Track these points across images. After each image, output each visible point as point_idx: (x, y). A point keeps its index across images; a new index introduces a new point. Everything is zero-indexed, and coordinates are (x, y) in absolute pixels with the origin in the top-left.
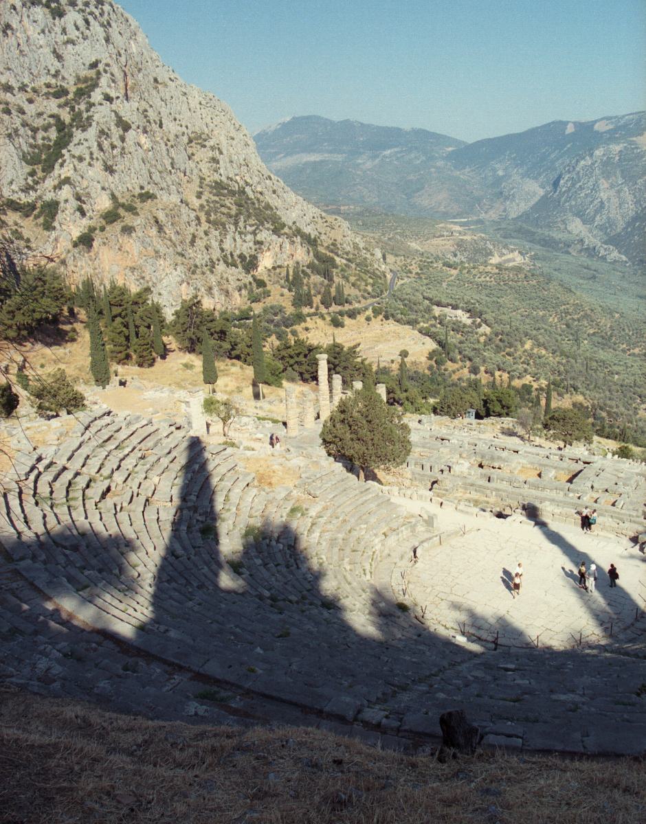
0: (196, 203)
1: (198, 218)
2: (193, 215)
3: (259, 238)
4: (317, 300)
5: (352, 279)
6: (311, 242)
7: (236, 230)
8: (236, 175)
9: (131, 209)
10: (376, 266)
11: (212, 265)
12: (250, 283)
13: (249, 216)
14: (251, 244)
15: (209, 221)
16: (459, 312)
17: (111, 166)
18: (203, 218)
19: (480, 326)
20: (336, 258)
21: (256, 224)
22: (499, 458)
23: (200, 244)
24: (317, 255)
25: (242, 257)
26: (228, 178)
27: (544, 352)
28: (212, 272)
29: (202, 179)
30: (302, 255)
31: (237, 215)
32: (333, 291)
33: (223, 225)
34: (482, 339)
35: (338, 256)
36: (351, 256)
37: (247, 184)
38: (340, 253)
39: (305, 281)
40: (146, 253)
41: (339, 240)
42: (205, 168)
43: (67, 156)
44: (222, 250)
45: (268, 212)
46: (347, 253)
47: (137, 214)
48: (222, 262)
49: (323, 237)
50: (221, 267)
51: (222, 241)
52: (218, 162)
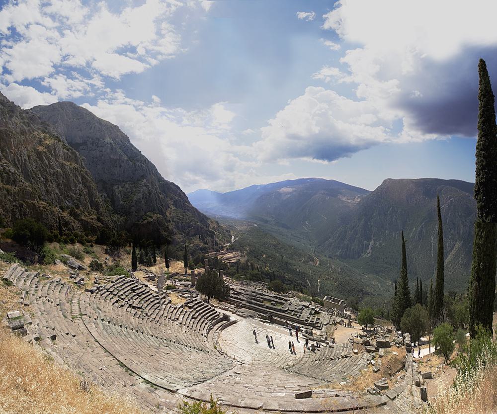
5: (220, 238)
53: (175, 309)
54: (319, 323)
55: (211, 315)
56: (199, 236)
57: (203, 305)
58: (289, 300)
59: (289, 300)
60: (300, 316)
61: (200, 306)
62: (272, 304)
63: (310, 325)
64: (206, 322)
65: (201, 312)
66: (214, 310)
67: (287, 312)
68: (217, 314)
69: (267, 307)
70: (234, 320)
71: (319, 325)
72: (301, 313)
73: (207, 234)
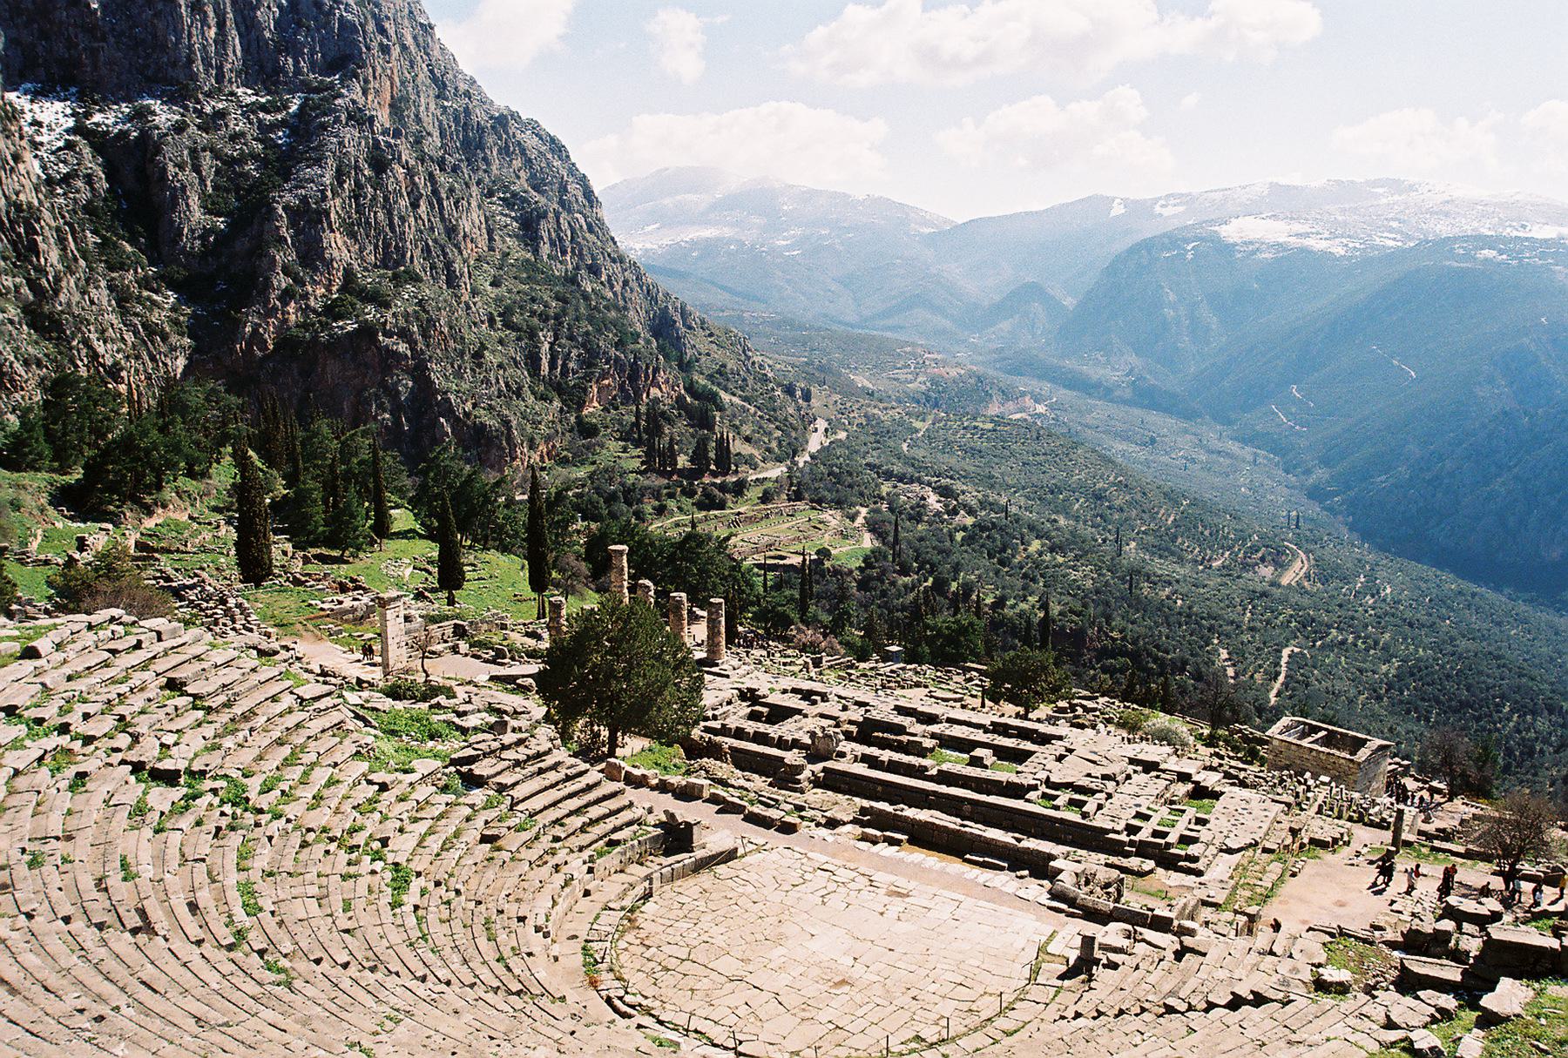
1: (492, 321)
4: (682, 461)
5: (747, 430)
6: (685, 366)
7: (556, 337)
8: (564, 253)
10: (791, 410)
13: (577, 319)
15: (508, 325)
19: (954, 512)
20: (722, 394)
21: (587, 333)
22: (901, 730)
24: (690, 389)
27: (1060, 560)
31: (556, 317)
33: (532, 334)
34: (959, 536)
35: (726, 390)
49: (703, 359)
50: (531, 399)
53: (384, 787)
54: (1195, 840)
55: (593, 822)
56: (638, 414)
57: (555, 767)
58: (1060, 738)
59: (1060, 738)
60: (1100, 807)
61: (541, 771)
62: (976, 762)
63: (1143, 850)
64: (561, 856)
65: (537, 803)
66: (621, 792)
67: (1032, 795)
68: (626, 816)
69: (945, 778)
70: (727, 845)
71: (1193, 850)
72: (1109, 796)
73: (680, 400)
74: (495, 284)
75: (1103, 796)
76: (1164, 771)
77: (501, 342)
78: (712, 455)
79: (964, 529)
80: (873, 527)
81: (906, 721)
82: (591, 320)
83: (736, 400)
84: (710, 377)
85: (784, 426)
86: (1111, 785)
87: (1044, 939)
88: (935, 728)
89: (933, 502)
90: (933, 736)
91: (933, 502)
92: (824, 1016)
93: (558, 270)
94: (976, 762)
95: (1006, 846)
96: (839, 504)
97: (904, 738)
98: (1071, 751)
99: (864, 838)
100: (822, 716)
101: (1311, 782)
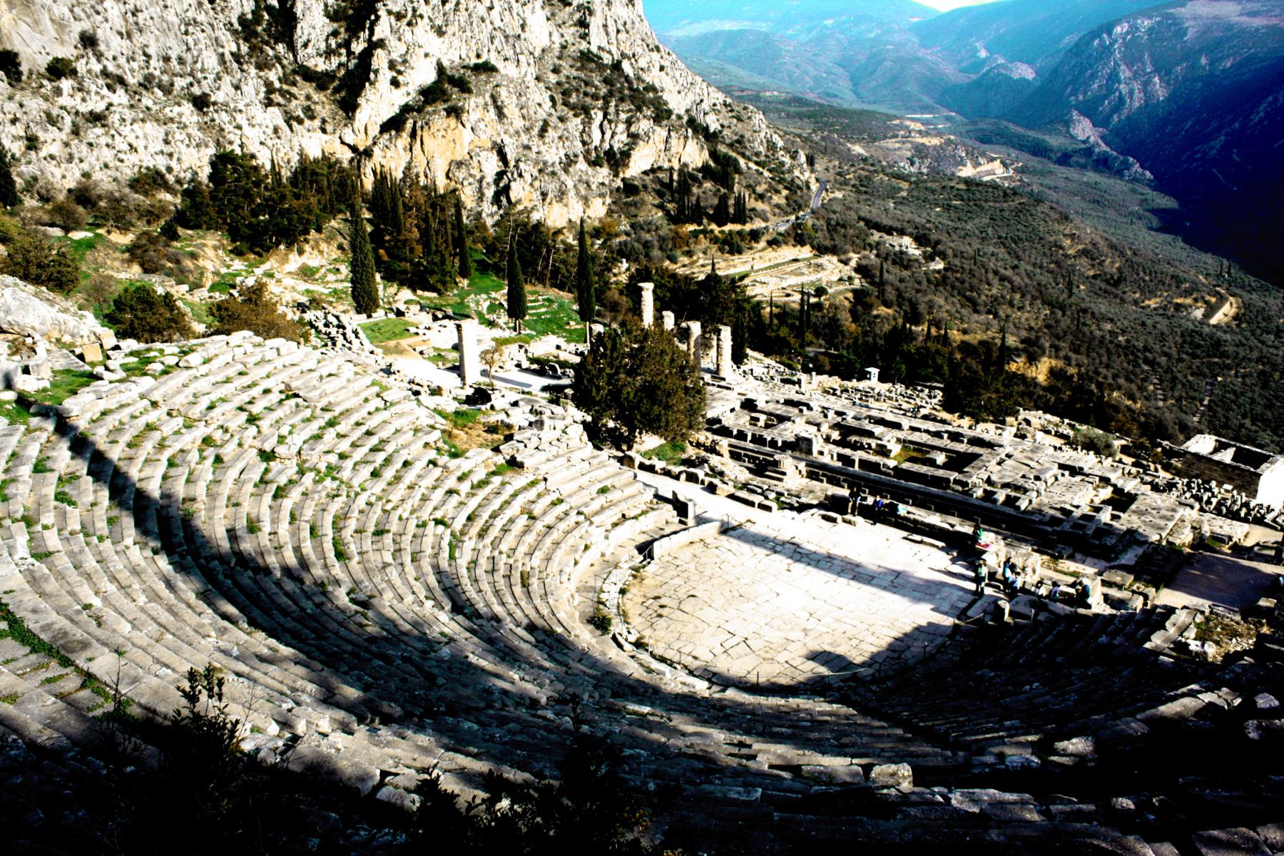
0: (553, 78)
1: (552, 99)
2: (547, 95)
3: (633, 129)
5: (760, 189)
6: (710, 138)
9: (463, 86)
10: (797, 173)
11: (569, 162)
12: (618, 189)
13: (622, 100)
14: (624, 138)
15: (565, 104)
16: (907, 241)
17: (440, 27)
18: (559, 102)
19: (930, 258)
20: (742, 162)
21: (630, 111)
22: (870, 434)
23: (551, 134)
24: (714, 154)
25: (610, 154)
26: (600, 48)
28: (566, 171)
29: (564, 47)
30: (694, 155)
31: (604, 98)
32: (731, 202)
33: (586, 110)
35: (743, 155)
36: (763, 158)
37: (623, 55)
38: (747, 153)
39: (695, 190)
40: (479, 144)
41: (748, 135)
42: (570, 32)
43: (382, 13)
44: (584, 143)
45: (651, 95)
46: (757, 154)
47: (469, 91)
48: (581, 158)
49: (725, 132)
50: (582, 165)
51: (584, 131)
52: (586, 26)
58: (1001, 446)
59: (1001, 446)
74: (556, 70)
75: (1035, 494)
76: (1087, 475)
77: (562, 119)
78: (731, 210)
79: (939, 272)
80: (861, 269)
81: (878, 430)
82: (632, 99)
83: (752, 165)
84: (731, 146)
85: (792, 187)
86: (1040, 485)
87: (965, 605)
88: (901, 435)
89: (914, 250)
90: (899, 440)
91: (914, 250)
92: (782, 658)
93: (607, 60)
94: (932, 463)
95: (941, 529)
96: (833, 250)
97: (874, 443)
98: (1009, 456)
99: (825, 518)
100: (808, 422)
101: (1216, 490)
